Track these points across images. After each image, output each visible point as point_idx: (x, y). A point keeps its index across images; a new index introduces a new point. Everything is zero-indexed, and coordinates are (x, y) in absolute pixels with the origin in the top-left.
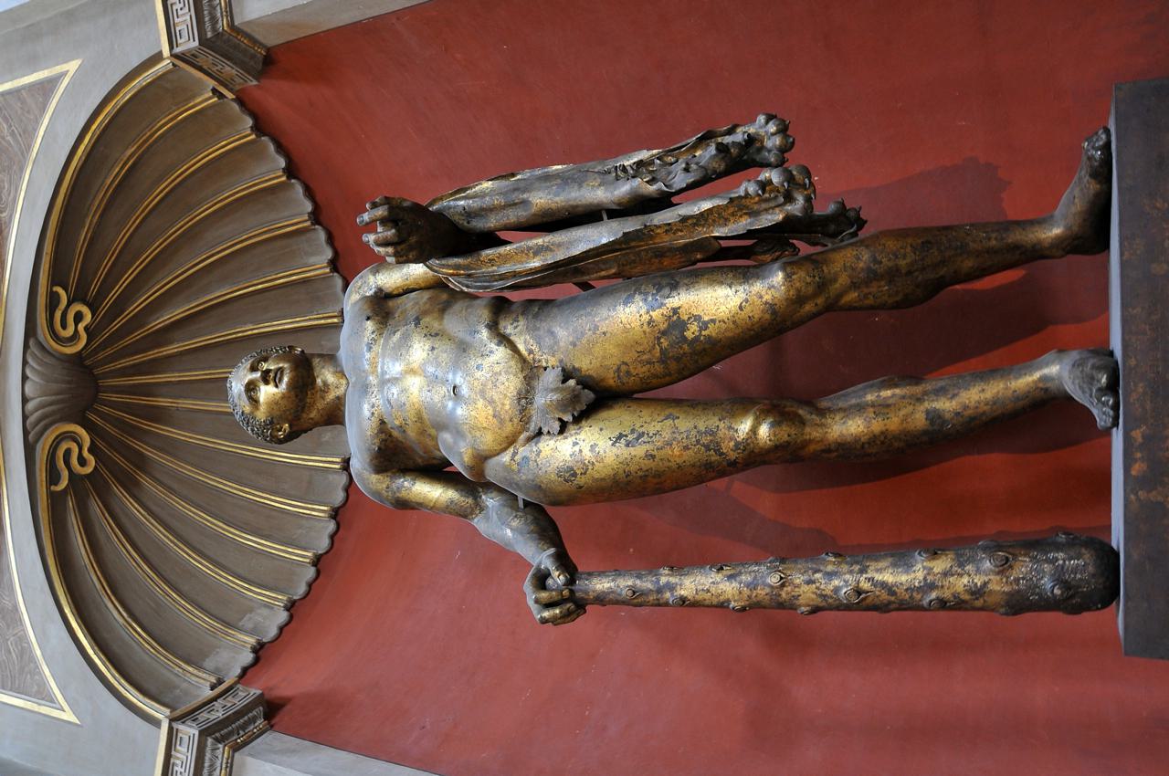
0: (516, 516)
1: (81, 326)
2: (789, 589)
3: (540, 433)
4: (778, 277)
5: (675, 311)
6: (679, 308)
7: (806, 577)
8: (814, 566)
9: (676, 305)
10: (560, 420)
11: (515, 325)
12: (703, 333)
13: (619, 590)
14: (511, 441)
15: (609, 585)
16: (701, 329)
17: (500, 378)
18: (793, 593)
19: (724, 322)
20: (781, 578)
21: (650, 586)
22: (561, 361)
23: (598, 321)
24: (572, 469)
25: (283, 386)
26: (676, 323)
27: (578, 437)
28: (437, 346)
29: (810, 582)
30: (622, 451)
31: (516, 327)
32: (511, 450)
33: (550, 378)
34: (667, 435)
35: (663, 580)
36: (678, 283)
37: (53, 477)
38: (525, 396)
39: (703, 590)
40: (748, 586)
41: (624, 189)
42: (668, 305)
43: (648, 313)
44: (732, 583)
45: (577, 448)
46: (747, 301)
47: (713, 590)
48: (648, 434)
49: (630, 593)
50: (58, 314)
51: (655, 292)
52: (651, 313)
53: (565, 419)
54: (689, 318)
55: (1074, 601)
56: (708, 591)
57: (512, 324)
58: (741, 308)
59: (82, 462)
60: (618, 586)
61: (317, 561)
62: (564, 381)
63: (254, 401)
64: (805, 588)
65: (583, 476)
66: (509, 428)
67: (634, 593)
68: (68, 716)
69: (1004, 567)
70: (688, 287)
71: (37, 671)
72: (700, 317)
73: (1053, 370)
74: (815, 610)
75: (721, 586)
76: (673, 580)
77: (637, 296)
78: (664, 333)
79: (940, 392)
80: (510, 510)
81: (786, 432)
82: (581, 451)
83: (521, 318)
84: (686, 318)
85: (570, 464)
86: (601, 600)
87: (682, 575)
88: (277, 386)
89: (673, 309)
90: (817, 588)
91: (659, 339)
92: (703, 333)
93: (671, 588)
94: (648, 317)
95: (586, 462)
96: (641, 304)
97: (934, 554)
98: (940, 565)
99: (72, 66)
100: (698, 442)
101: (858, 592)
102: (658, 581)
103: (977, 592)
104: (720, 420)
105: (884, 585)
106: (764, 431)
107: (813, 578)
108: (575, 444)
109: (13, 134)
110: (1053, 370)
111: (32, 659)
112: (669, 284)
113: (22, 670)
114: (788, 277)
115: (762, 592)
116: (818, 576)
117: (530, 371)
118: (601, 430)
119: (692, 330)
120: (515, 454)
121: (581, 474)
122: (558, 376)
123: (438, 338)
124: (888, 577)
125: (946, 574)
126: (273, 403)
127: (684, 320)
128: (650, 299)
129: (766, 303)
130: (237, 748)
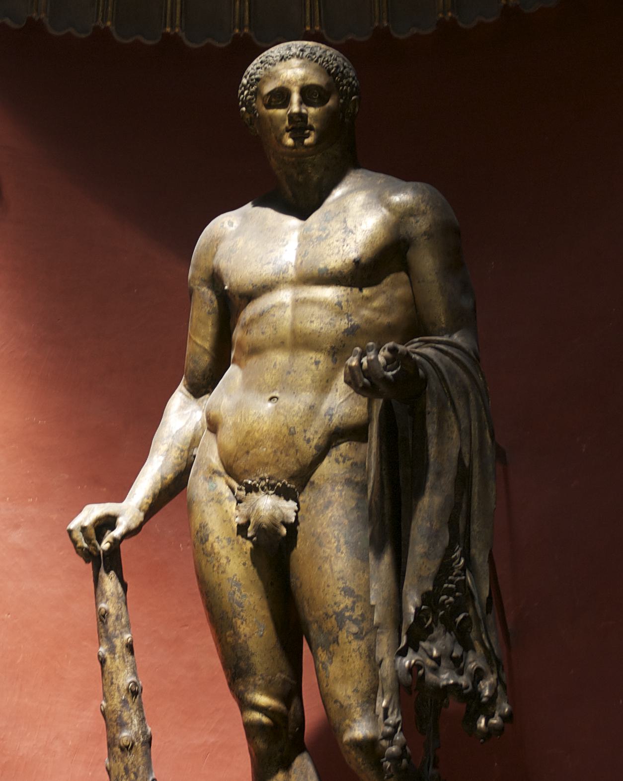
0: (182, 451)
2: (120, 753)
3: (239, 502)
5: (336, 641)
6: (338, 644)
7: (130, 767)
8: (141, 772)
9: (340, 641)
10: (248, 523)
11: (341, 459)
12: (320, 665)
13: (104, 600)
15: (108, 590)
16: (323, 663)
17: (284, 455)
18: (117, 757)
19: (327, 686)
20: (127, 747)
21: (111, 629)
22: (303, 517)
23: (330, 561)
24: (207, 540)
27: (236, 542)
28: (320, 367)
29: (126, 770)
31: (337, 461)
32: (221, 469)
35: (118, 643)
36: (362, 639)
39: (112, 678)
40: (120, 717)
42: (340, 632)
43: (335, 613)
44: (120, 703)
45: (225, 542)
46: (342, 706)
47: (114, 687)
48: (242, 611)
49: (103, 610)
51: (354, 617)
52: (334, 616)
53: (249, 529)
54: (330, 653)
56: (112, 683)
57: (341, 455)
58: (336, 702)
60: (107, 600)
61: (170, 41)
62: (284, 523)
64: (122, 767)
65: (202, 552)
67: (104, 616)
72: (331, 663)
75: (117, 694)
76: (118, 649)
77: (351, 599)
78: (320, 627)
80: (189, 440)
82: (223, 547)
83: (349, 463)
84: (331, 649)
85: (211, 539)
87: (123, 657)
88: (287, 130)
89: (337, 637)
90: (122, 777)
91: (317, 622)
92: (320, 665)
93: (112, 650)
94: (330, 612)
95: (213, 555)
96: (342, 606)
100: (240, 658)
102: (117, 637)
104: (261, 675)
107: (130, 772)
108: (229, 540)
112: (361, 630)
116: (132, 776)
118: (244, 564)
120: (220, 474)
121: (203, 549)
122: (287, 517)
123: (331, 365)
127: (329, 647)
128: (347, 614)
129: (340, 724)
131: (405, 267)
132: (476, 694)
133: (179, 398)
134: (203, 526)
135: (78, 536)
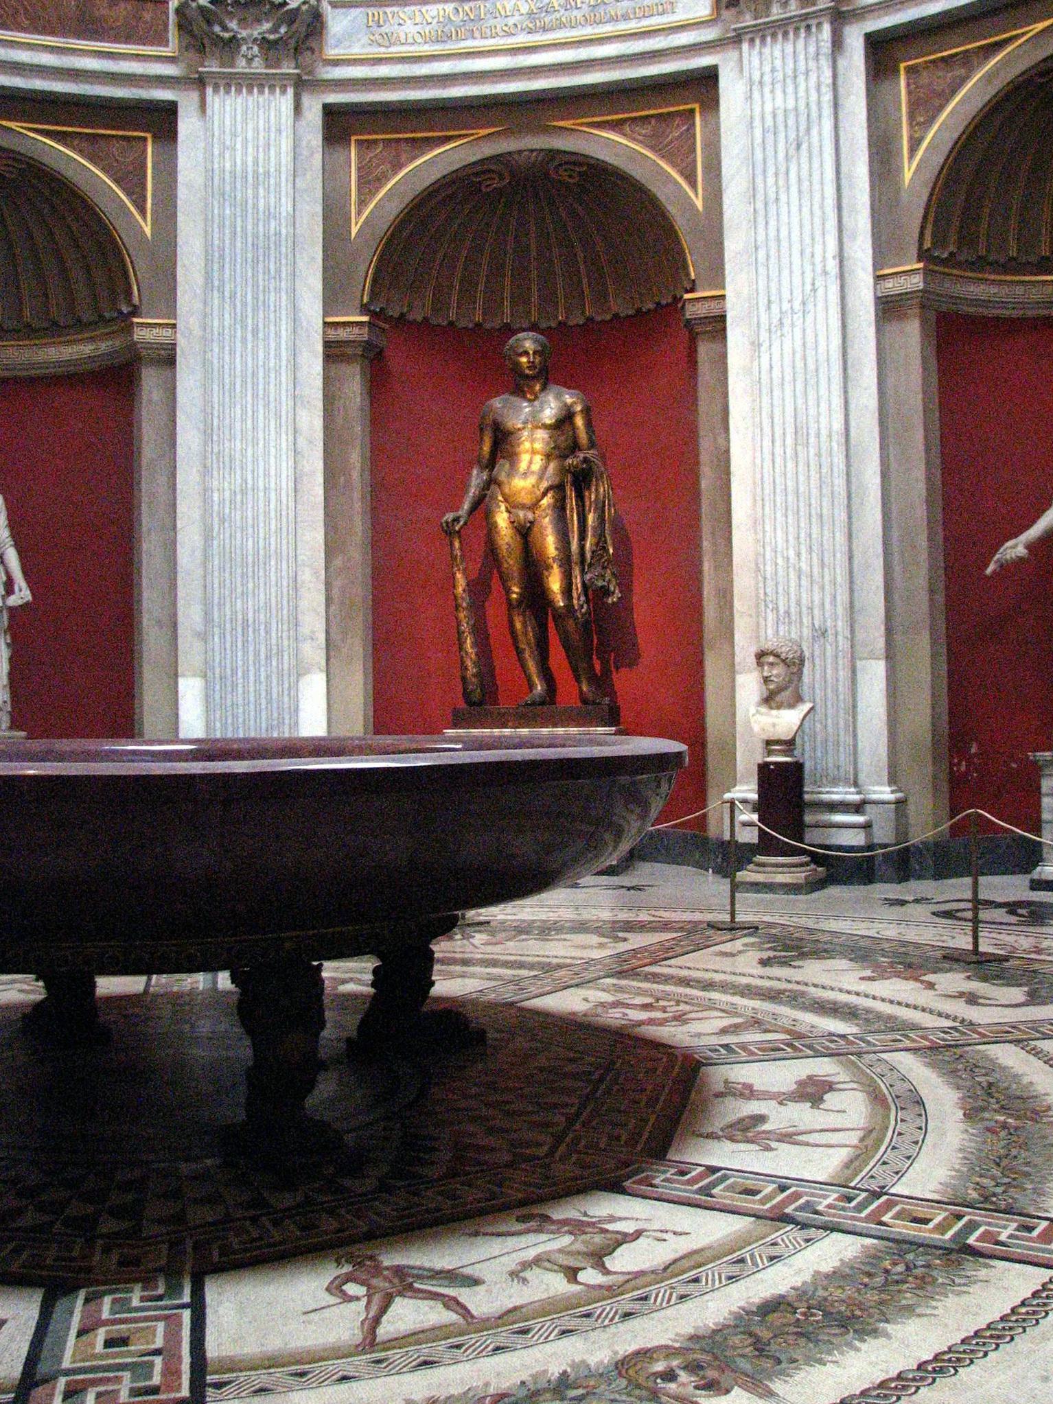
1: (566, 178)
4: (562, 604)
14: (506, 500)
25: (527, 372)
26: (548, 568)
30: (504, 547)
33: (530, 516)
34: (511, 562)
37: (476, 174)
38: (523, 507)
41: (588, 555)
50: (572, 167)
55: (466, 695)
59: (487, 186)
63: (521, 355)
66: (511, 500)
68: (354, 231)
69: (474, 676)
70: (561, 572)
71: (372, 194)
73: (539, 688)
74: (457, 618)
79: (532, 652)
81: (514, 603)
86: (452, 544)
97: (477, 654)
98: (473, 656)
99: (699, 204)
101: (463, 632)
103: (466, 668)
105: (465, 642)
106: (515, 596)
109: (672, 142)
110: (539, 688)
111: (377, 189)
113: (369, 182)
114: (560, 607)
115: (460, 601)
117: (534, 506)
119: (546, 573)
124: (468, 641)
125: (471, 659)
126: (518, 364)
130: (362, 355)
131: (572, 424)
132: (608, 589)
133: (475, 472)
134: (496, 522)
135: (444, 525)
